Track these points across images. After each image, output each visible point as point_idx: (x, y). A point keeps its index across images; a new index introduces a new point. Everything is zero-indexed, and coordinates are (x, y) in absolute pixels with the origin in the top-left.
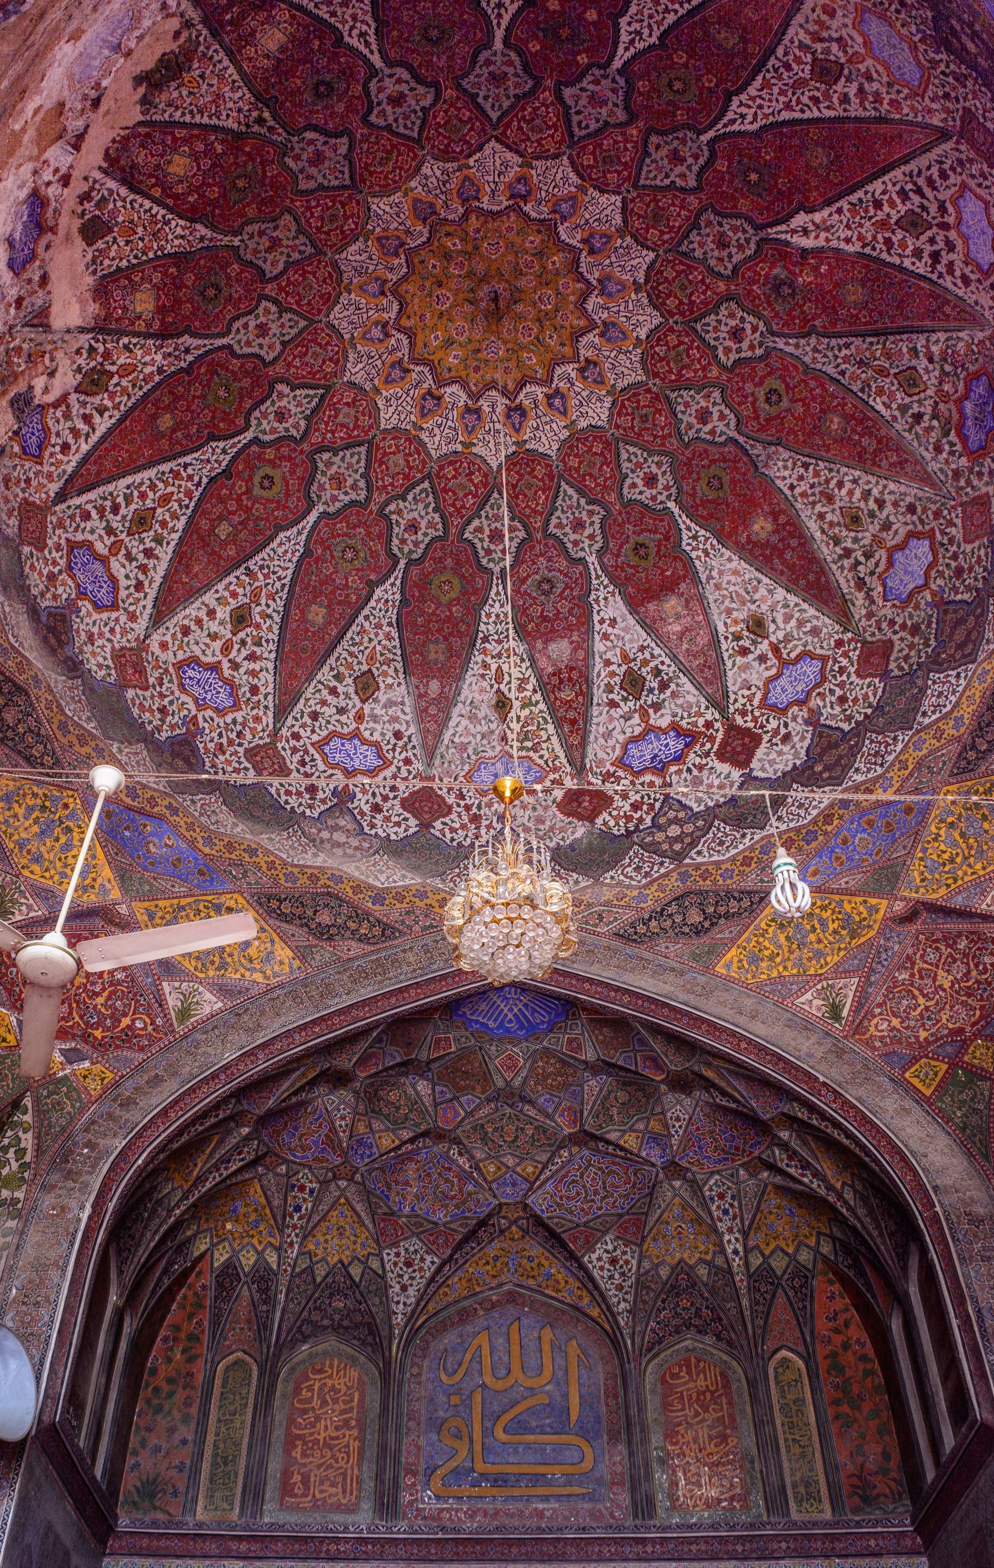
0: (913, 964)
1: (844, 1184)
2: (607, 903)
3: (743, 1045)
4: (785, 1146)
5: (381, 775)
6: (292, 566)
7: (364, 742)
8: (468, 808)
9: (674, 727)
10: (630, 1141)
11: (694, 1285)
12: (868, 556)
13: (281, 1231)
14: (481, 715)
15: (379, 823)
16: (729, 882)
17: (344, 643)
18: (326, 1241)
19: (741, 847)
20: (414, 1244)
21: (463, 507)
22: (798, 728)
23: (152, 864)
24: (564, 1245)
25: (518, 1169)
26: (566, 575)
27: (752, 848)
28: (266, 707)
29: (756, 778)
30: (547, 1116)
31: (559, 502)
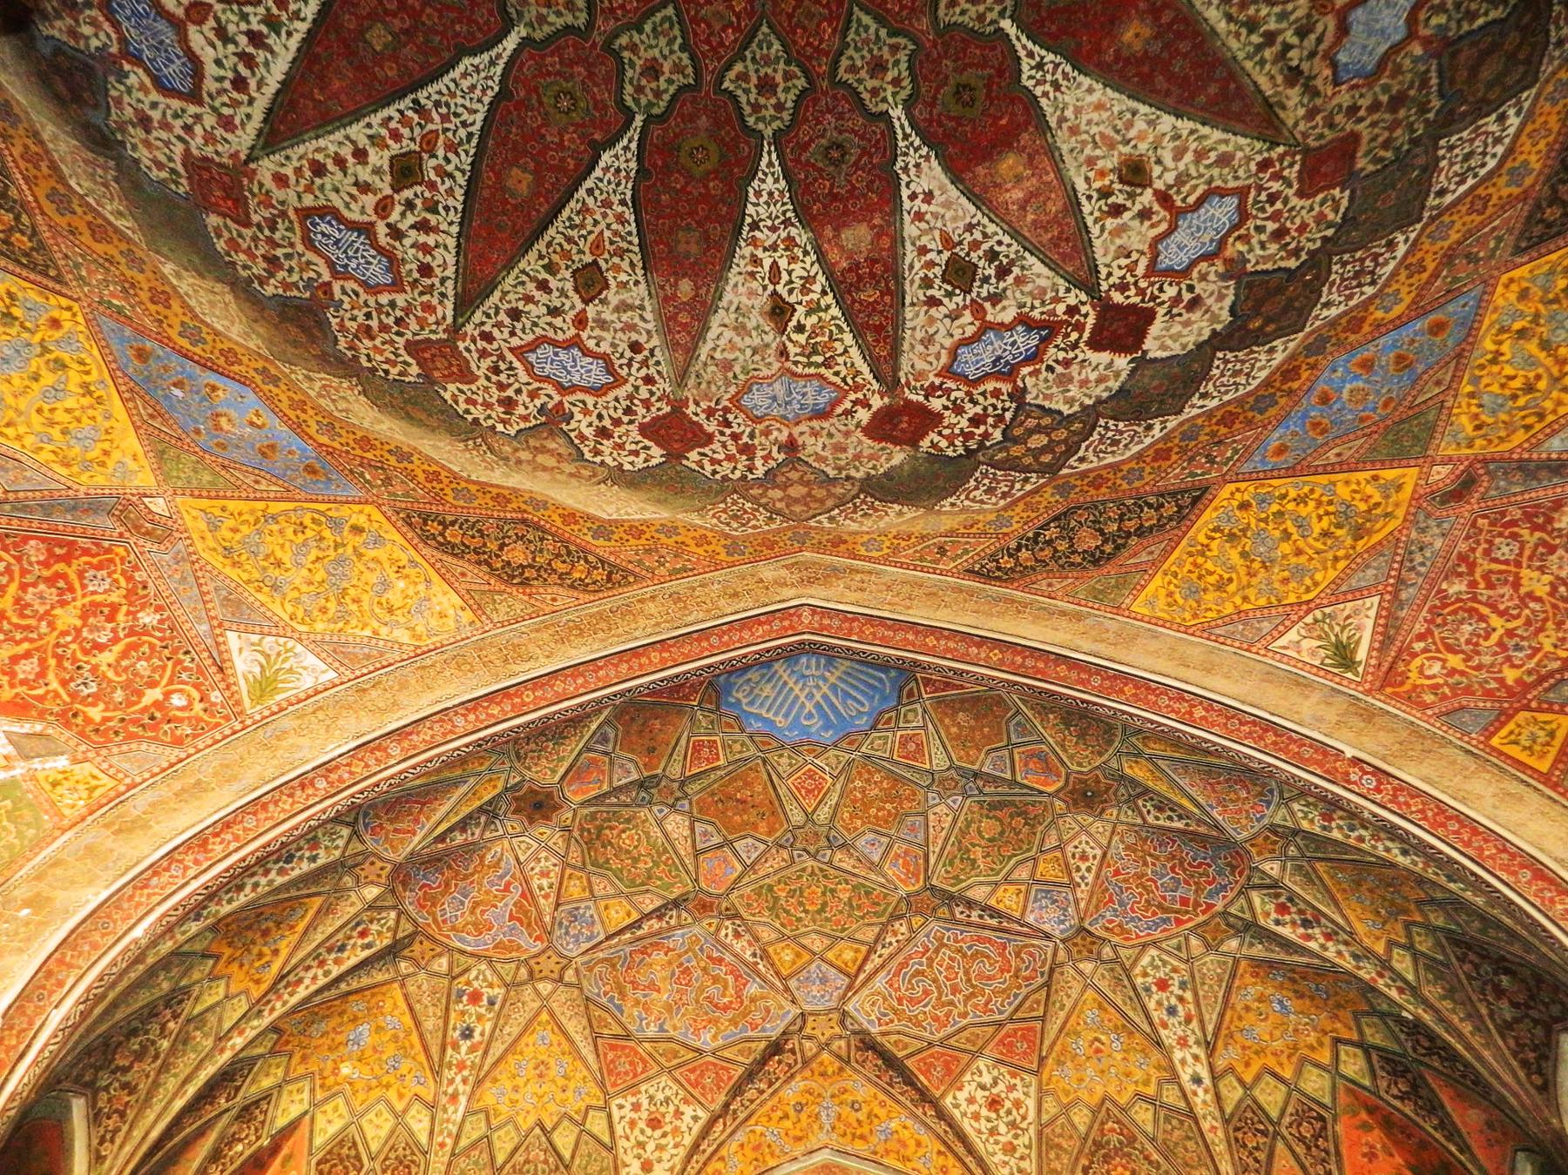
0: (1472, 566)
1: (1391, 944)
2: (951, 533)
3: (1199, 712)
4: (1272, 887)
5: (611, 396)
6: (483, 110)
7: (586, 352)
8: (735, 437)
9: (1024, 320)
10: (1008, 900)
11: (1132, 1139)
12: (1302, 33)
13: (437, 1074)
14: (750, 325)
15: (607, 452)
16: (1137, 484)
17: (560, 223)
18: (516, 1089)
19: (1148, 441)
20: (662, 1088)
21: (721, 44)
22: (1212, 287)
23: (222, 446)
24: (909, 1080)
25: (830, 955)
26: (862, 138)
27: (1167, 438)
28: (443, 295)
29: (1155, 360)
30: (873, 867)
31: (851, 36)
